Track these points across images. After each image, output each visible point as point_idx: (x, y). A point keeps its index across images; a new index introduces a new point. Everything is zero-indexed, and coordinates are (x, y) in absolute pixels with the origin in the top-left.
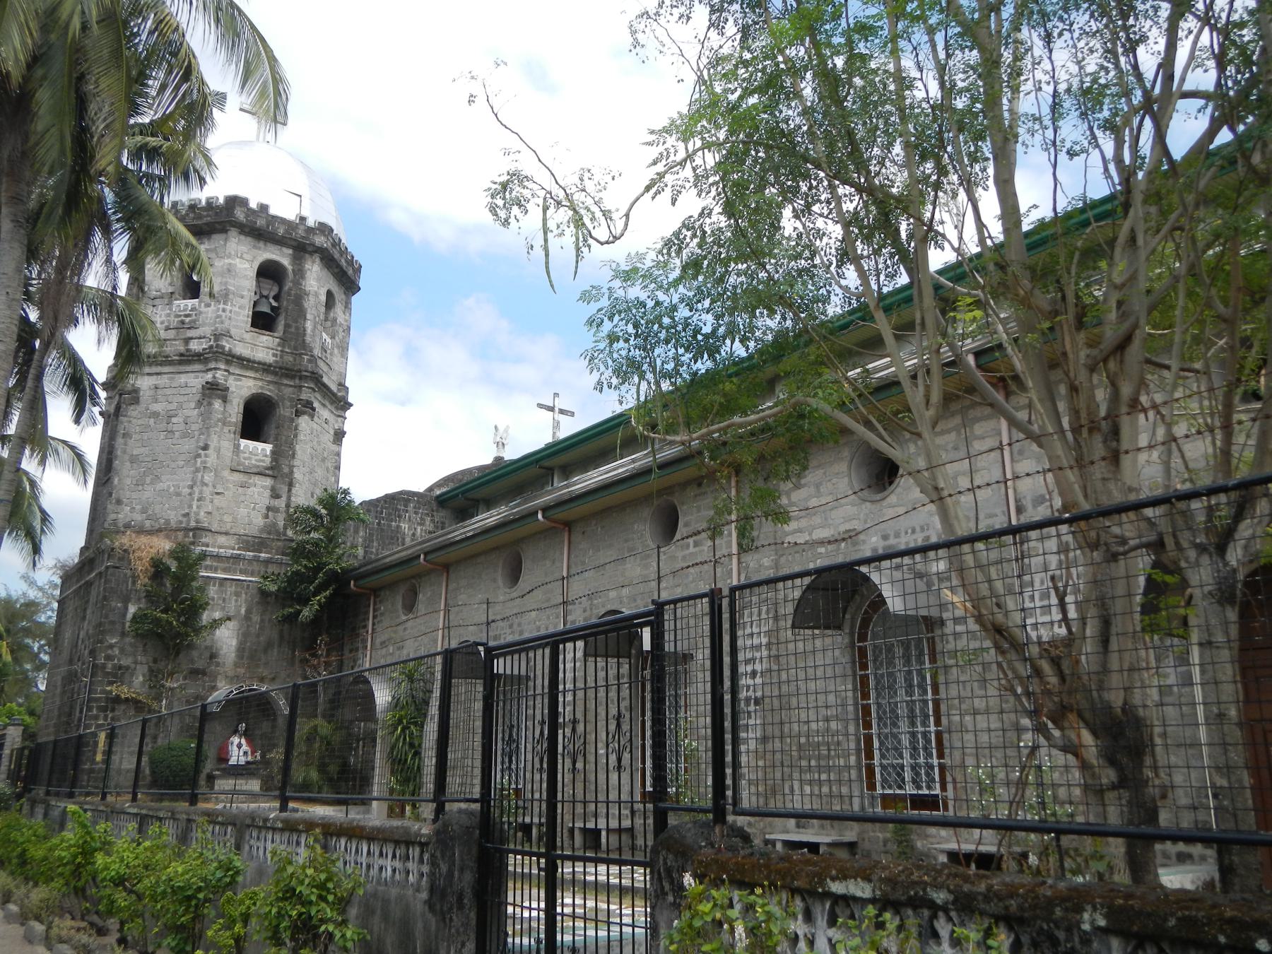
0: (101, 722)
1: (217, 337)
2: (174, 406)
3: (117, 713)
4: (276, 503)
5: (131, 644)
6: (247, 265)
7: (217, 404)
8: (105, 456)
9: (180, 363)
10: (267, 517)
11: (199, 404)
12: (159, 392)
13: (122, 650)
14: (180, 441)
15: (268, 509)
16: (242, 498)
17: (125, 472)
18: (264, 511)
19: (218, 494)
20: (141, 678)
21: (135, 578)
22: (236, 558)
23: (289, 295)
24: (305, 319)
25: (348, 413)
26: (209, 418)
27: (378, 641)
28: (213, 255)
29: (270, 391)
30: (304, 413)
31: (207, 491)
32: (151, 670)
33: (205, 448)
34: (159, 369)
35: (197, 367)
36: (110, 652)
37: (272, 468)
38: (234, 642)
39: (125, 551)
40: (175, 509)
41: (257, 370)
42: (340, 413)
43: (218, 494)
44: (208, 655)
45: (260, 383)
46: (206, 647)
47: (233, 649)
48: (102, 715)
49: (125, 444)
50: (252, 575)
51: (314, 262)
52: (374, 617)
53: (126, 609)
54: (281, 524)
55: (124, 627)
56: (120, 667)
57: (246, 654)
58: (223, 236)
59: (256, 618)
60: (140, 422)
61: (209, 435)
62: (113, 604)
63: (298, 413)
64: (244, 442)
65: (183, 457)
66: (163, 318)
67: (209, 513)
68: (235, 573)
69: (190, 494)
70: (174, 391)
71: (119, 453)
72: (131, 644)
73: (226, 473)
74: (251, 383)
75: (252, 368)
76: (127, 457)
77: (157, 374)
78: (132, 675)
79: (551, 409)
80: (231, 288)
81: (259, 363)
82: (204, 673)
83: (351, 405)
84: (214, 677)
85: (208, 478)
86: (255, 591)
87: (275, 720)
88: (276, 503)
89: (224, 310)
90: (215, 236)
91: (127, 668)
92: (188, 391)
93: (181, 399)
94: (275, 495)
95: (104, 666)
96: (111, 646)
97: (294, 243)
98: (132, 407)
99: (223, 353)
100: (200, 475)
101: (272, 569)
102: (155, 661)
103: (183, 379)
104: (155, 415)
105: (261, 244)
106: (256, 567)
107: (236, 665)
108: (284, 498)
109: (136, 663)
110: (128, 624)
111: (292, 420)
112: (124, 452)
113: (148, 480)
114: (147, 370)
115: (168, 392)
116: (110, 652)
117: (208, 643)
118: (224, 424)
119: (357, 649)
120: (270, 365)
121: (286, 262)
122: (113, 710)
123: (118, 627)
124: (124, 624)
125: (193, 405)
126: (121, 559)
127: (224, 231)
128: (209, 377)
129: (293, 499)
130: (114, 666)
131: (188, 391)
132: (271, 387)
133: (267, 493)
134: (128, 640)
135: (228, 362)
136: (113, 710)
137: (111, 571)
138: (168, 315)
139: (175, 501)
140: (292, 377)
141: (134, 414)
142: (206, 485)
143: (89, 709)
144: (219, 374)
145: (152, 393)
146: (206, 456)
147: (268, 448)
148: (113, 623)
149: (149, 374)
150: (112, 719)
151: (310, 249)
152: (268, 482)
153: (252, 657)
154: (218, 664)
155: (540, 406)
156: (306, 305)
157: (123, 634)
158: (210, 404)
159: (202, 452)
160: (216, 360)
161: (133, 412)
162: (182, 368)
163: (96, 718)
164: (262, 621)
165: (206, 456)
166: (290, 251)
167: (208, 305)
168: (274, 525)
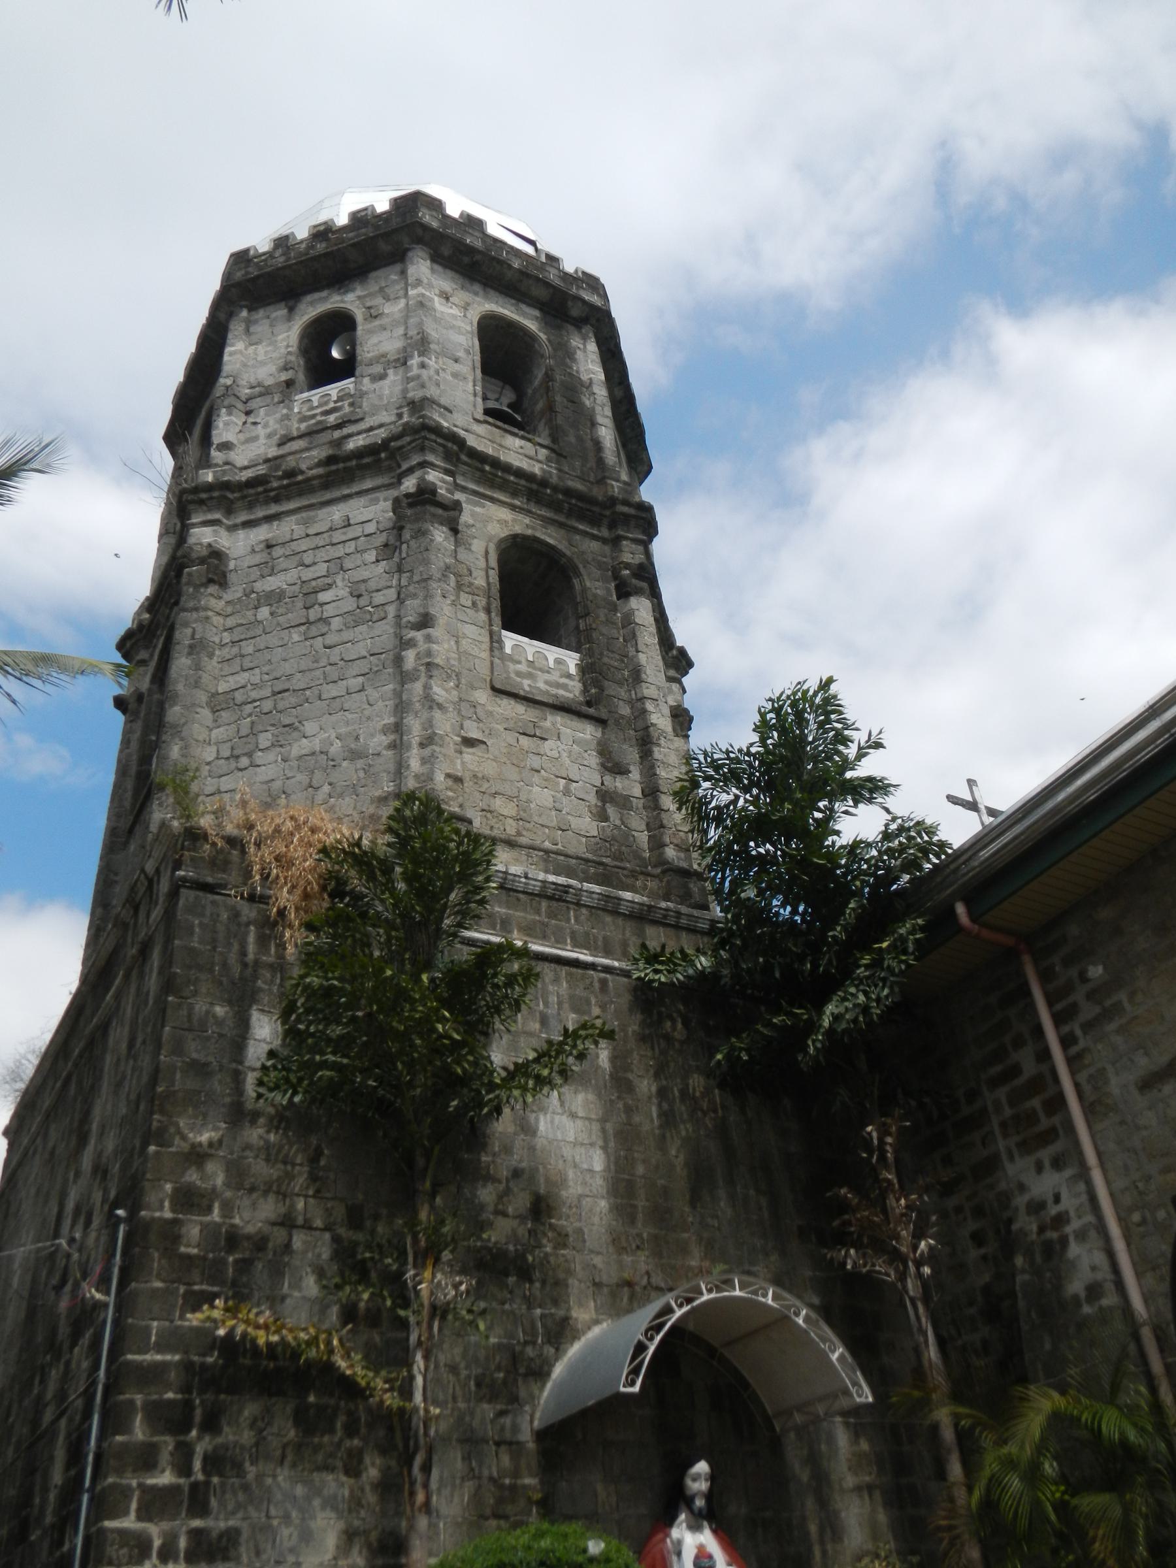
0: (165, 1478)
1: (416, 406)
2: (322, 569)
3: (228, 1435)
4: (618, 784)
5: (269, 1154)
6: (455, 311)
7: (439, 535)
8: (130, 784)
9: (328, 483)
10: (602, 816)
11: (388, 551)
12: (278, 552)
13: (237, 1174)
14: (347, 635)
15: (605, 796)
16: (535, 762)
17: (198, 731)
18: (592, 798)
19: (469, 742)
20: (311, 1286)
21: (270, 926)
22: (556, 896)
23: (548, 377)
24: (594, 424)
25: (685, 680)
26: (426, 562)
27: (1119, 1083)
28: (378, 301)
29: (551, 537)
30: (638, 592)
31: (444, 724)
32: (344, 1253)
33: (425, 622)
34: (274, 509)
35: (368, 484)
36: (192, 1176)
37: (589, 704)
38: (598, 1162)
39: (232, 841)
40: (354, 789)
41: (514, 494)
42: (672, 673)
43: (469, 742)
44: (520, 1202)
45: (527, 520)
46: (516, 1173)
47: (598, 1184)
48: (168, 1443)
49: (198, 667)
50: (608, 953)
51: (585, 338)
52: (1059, 1020)
53: (243, 1025)
54: (643, 838)
55: (239, 1089)
56: (233, 1239)
57: (641, 1203)
58: (398, 267)
59: (646, 1086)
60: (230, 622)
61: (428, 596)
62: (200, 1006)
63: (624, 592)
64: (511, 639)
65: (362, 666)
66: (273, 424)
67: (458, 780)
68: (559, 942)
69: (393, 746)
70: (319, 541)
71: (180, 687)
72: (269, 1154)
73: (482, 696)
74: (504, 514)
75: (503, 486)
76: (203, 697)
77: (269, 519)
78: (277, 1271)
79: (973, 806)
80: (433, 334)
81: (519, 473)
82: (525, 1273)
83: (690, 664)
84: (556, 1289)
85: (439, 692)
86: (625, 1000)
87: (776, 1444)
88: (618, 784)
89: (423, 366)
90: (373, 274)
91: (260, 1243)
92: (352, 533)
93: (340, 551)
94: (614, 767)
95: (171, 1233)
96: (197, 1156)
97: (541, 293)
98: (212, 589)
99: (437, 430)
100: (417, 687)
101: (655, 938)
102: (355, 1218)
103: (336, 513)
104: (274, 598)
105: (477, 287)
106: (612, 929)
107: (619, 1243)
108: (635, 774)
109: (287, 1222)
110: (251, 1079)
111: (614, 608)
112: (197, 684)
113: (265, 740)
114: (243, 517)
115: (303, 545)
116: (192, 1176)
117: (519, 1158)
118: (459, 587)
119: (991, 1165)
120: (543, 483)
121: (532, 325)
122: (211, 1425)
123: (219, 1085)
124: (237, 1078)
125: (371, 556)
126: (219, 862)
127: (399, 257)
128: (409, 484)
129: (662, 772)
130: (211, 1232)
131: (352, 533)
132: (552, 530)
133: (593, 760)
134: (255, 1134)
135: (448, 456)
136: (211, 1425)
137: (187, 896)
138: (287, 417)
139: (349, 771)
140: (595, 522)
141: (219, 605)
142: (440, 706)
143: (114, 1420)
144: (433, 476)
145: (258, 559)
146: (429, 639)
147: (572, 660)
148: (200, 1069)
149: (248, 524)
150: (213, 1462)
151: (575, 312)
152: (588, 732)
153: (660, 1215)
154: (562, 1240)
155: (953, 800)
156: (587, 403)
157: (239, 1115)
158: (421, 533)
159: (418, 635)
160: (422, 449)
161: (214, 601)
162: (328, 496)
163: (147, 1460)
164: (662, 1093)
165: (429, 639)
166: (537, 313)
167: (382, 377)
168: (625, 837)
